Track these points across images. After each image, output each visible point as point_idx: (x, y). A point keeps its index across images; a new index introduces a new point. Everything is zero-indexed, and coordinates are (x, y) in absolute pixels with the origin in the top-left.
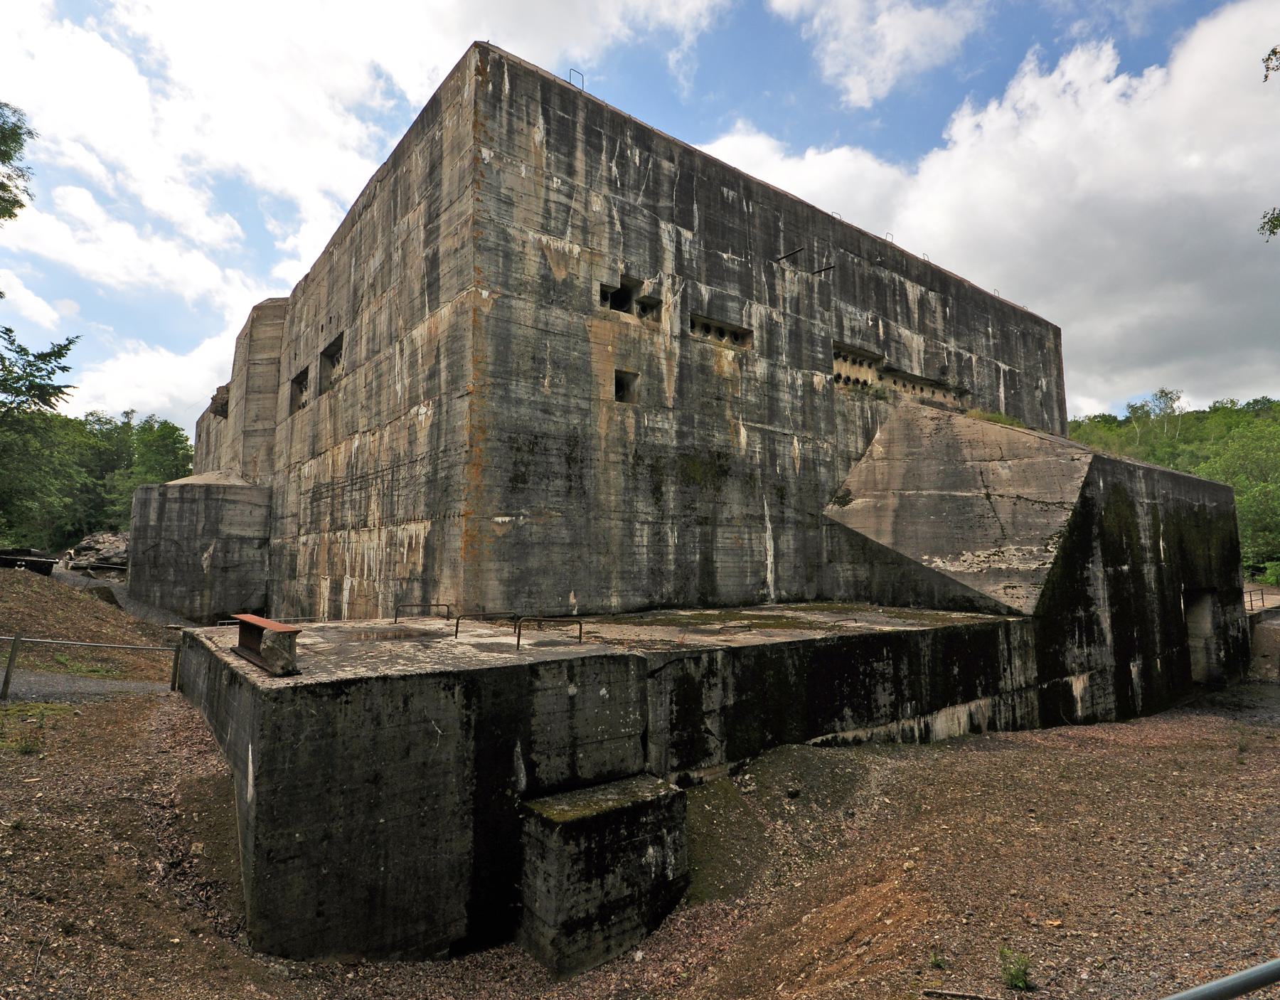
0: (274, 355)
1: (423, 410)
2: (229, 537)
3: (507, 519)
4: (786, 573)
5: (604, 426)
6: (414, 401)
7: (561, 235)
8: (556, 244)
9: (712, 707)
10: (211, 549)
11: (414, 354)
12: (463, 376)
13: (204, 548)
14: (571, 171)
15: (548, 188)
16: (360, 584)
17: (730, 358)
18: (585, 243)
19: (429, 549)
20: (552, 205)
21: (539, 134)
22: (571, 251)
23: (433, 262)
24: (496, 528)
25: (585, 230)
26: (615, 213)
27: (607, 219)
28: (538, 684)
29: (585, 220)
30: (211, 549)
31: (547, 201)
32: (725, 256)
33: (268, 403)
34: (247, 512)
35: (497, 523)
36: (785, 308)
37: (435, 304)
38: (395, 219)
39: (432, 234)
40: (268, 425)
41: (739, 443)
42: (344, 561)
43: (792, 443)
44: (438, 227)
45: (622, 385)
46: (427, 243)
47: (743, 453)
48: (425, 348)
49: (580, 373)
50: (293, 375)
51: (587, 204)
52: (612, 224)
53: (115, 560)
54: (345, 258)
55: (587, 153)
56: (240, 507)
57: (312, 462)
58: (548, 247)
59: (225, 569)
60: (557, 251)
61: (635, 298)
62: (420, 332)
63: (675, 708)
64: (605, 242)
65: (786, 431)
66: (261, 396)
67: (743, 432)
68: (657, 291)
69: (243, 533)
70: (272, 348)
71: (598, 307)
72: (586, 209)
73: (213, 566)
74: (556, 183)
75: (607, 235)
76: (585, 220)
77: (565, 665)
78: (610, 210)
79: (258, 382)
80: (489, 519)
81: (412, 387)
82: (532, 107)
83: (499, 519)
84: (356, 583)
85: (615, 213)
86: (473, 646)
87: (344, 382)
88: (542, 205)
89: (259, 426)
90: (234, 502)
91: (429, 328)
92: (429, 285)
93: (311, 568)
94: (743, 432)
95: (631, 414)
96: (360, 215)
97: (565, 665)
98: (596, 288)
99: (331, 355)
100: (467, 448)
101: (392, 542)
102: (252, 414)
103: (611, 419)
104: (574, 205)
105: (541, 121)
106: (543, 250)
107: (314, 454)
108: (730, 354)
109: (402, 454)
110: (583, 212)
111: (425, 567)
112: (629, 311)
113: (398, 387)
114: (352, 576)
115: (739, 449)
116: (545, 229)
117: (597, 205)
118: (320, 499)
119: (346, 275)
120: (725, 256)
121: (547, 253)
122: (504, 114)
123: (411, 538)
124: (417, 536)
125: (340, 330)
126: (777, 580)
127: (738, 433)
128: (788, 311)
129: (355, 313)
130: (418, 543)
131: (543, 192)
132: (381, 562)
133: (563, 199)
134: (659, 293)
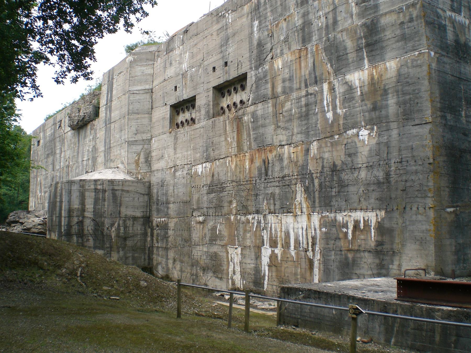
0: (147, 87)
2: (127, 218)
10: (116, 225)
13: (112, 225)
24: (447, 215)
30: (116, 225)
33: (146, 121)
34: (136, 199)
35: (448, 213)
40: (145, 136)
46: (361, 15)
48: (366, 89)
53: (33, 230)
57: (208, 165)
59: (125, 239)
66: (139, 116)
69: (134, 214)
70: (146, 82)
73: (118, 236)
79: (136, 106)
80: (444, 209)
83: (449, 210)
84: (278, 251)
89: (139, 137)
90: (128, 191)
100: (431, 161)
102: (133, 129)
123: (356, 224)
125: (241, 72)
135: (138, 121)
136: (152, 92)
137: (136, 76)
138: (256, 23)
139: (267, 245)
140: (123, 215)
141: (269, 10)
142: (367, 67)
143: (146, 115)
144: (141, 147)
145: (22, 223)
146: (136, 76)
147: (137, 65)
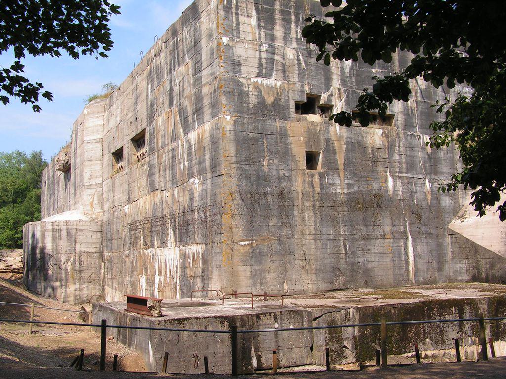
1: (197, 181)
3: (247, 243)
4: (422, 265)
5: (300, 185)
6: (191, 176)
7: (268, 76)
8: (266, 82)
9: (347, 335)
10: (72, 259)
11: (190, 147)
12: (219, 165)
13: (68, 260)
14: (272, 38)
15: (260, 51)
16: (165, 280)
17: (380, 134)
18: (285, 78)
19: (205, 261)
20: (264, 61)
21: (254, 21)
22: (276, 85)
23: (198, 98)
24: (241, 248)
25: (284, 71)
26: (301, 57)
27: (296, 62)
28: (261, 322)
29: (283, 65)
30: (72, 259)
31: (260, 59)
32: (373, 70)
35: (241, 245)
36: (417, 97)
37: (201, 122)
38: (175, 67)
39: (197, 82)
41: (387, 187)
42: (153, 267)
43: (425, 184)
44: (201, 78)
45: (311, 159)
46: (194, 85)
47: (391, 193)
49: (284, 154)
50: (113, 151)
51: (283, 56)
52: (299, 64)
54: (144, 83)
55: (284, 27)
56: (85, 233)
57: (129, 206)
58: (262, 85)
59: (80, 271)
60: (267, 85)
61: (317, 105)
62: (193, 136)
63: (327, 335)
64: (296, 76)
65: (420, 176)
66: (93, 163)
67: (390, 180)
68: (329, 100)
71: (293, 115)
72: (284, 59)
73: (73, 269)
74: (265, 47)
75: (297, 72)
76: (283, 65)
77: (273, 314)
78: (298, 56)
81: (190, 168)
82: (249, 7)
83: (242, 243)
84: (162, 278)
85: (301, 57)
86: (232, 308)
87: (147, 160)
88: (257, 61)
90: (81, 230)
91: (198, 134)
92: (197, 110)
93: (132, 272)
94: (390, 180)
95: (316, 176)
96: (152, 61)
97: (273, 314)
98: (292, 104)
99: (139, 141)
101: (184, 256)
103: (304, 180)
104: (276, 57)
105: (254, 13)
106: (257, 87)
107: (130, 201)
108: (380, 132)
109: (186, 206)
110: (282, 61)
111: (203, 272)
112: (314, 113)
113: (182, 166)
114: (160, 275)
115: (387, 191)
116: (260, 75)
117: (290, 53)
118: (135, 230)
119: (145, 94)
120: (373, 70)
121: (262, 89)
122: (234, 15)
123: (194, 253)
124: (198, 253)
126: (416, 270)
127: (386, 181)
128: (419, 99)
129: (151, 118)
130: (198, 256)
131: (258, 53)
132: (177, 267)
133: (270, 56)
134: (331, 101)
135: (92, 167)
136: (102, 141)
137: (90, 127)
138: (150, 86)
139: (157, 275)
140: (77, 251)
141: (155, 76)
142: (196, 128)
143: (99, 162)
144: (95, 190)
145: (5, 261)
146: (90, 127)
147: (90, 118)
